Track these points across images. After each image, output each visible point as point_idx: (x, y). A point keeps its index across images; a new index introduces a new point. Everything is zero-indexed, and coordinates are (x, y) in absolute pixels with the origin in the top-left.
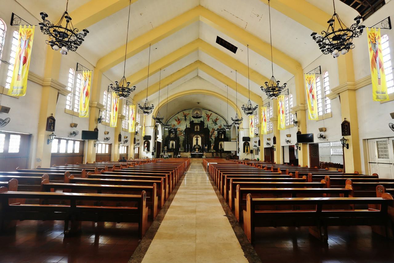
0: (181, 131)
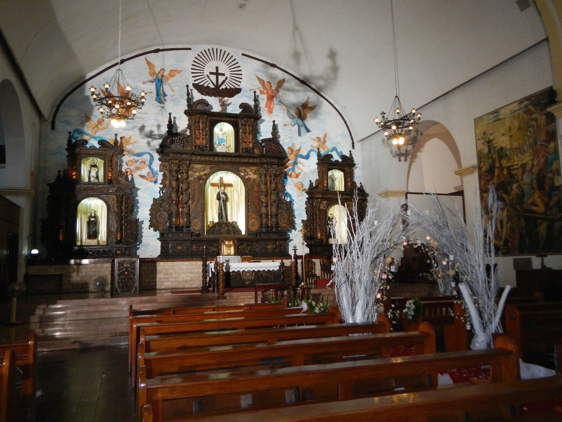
0: (139, 155)
